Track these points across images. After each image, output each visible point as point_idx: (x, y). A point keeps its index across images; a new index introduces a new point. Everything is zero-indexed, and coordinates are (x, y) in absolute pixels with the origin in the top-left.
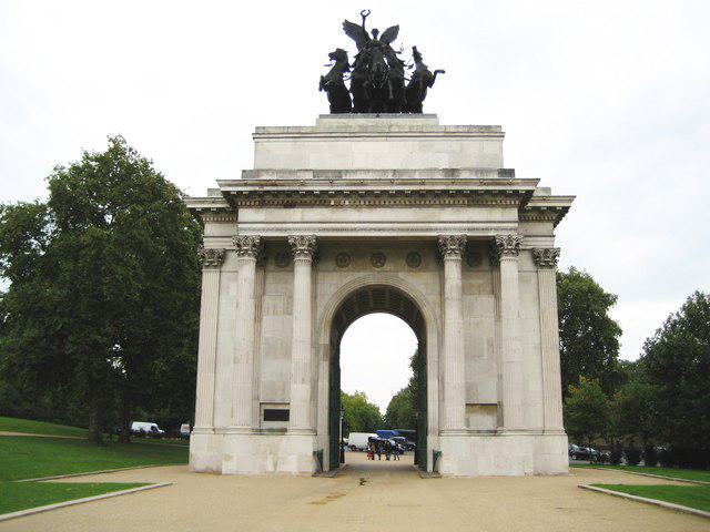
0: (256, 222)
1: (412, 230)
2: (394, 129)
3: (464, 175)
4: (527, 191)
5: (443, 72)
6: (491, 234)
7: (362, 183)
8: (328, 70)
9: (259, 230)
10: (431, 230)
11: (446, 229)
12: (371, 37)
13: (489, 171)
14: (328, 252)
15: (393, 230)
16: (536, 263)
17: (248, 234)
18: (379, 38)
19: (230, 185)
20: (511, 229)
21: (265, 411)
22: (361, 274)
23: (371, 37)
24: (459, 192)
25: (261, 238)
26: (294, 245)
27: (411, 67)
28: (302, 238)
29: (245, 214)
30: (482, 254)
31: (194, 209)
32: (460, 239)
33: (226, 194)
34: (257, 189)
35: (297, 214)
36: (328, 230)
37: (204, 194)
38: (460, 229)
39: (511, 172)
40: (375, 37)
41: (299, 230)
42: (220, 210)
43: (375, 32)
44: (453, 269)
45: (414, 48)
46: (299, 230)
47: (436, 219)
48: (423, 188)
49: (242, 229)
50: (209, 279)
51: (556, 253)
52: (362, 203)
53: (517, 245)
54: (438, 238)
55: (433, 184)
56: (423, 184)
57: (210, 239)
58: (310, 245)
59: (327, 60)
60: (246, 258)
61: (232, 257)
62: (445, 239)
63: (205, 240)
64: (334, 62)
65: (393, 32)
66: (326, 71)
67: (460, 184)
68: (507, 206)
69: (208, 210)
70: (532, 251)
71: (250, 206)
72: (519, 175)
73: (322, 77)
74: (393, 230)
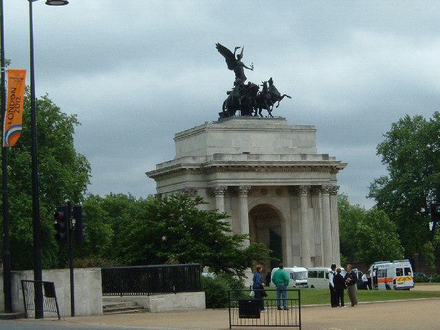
0: (223, 180)
3: (309, 159)
5: (290, 97)
7: (272, 162)
10: (295, 182)
12: (237, 58)
13: (316, 155)
14: (253, 191)
23: (237, 58)
30: (314, 190)
32: (308, 186)
34: (228, 164)
35: (242, 175)
39: (326, 156)
44: (304, 199)
45: (271, 79)
51: (338, 188)
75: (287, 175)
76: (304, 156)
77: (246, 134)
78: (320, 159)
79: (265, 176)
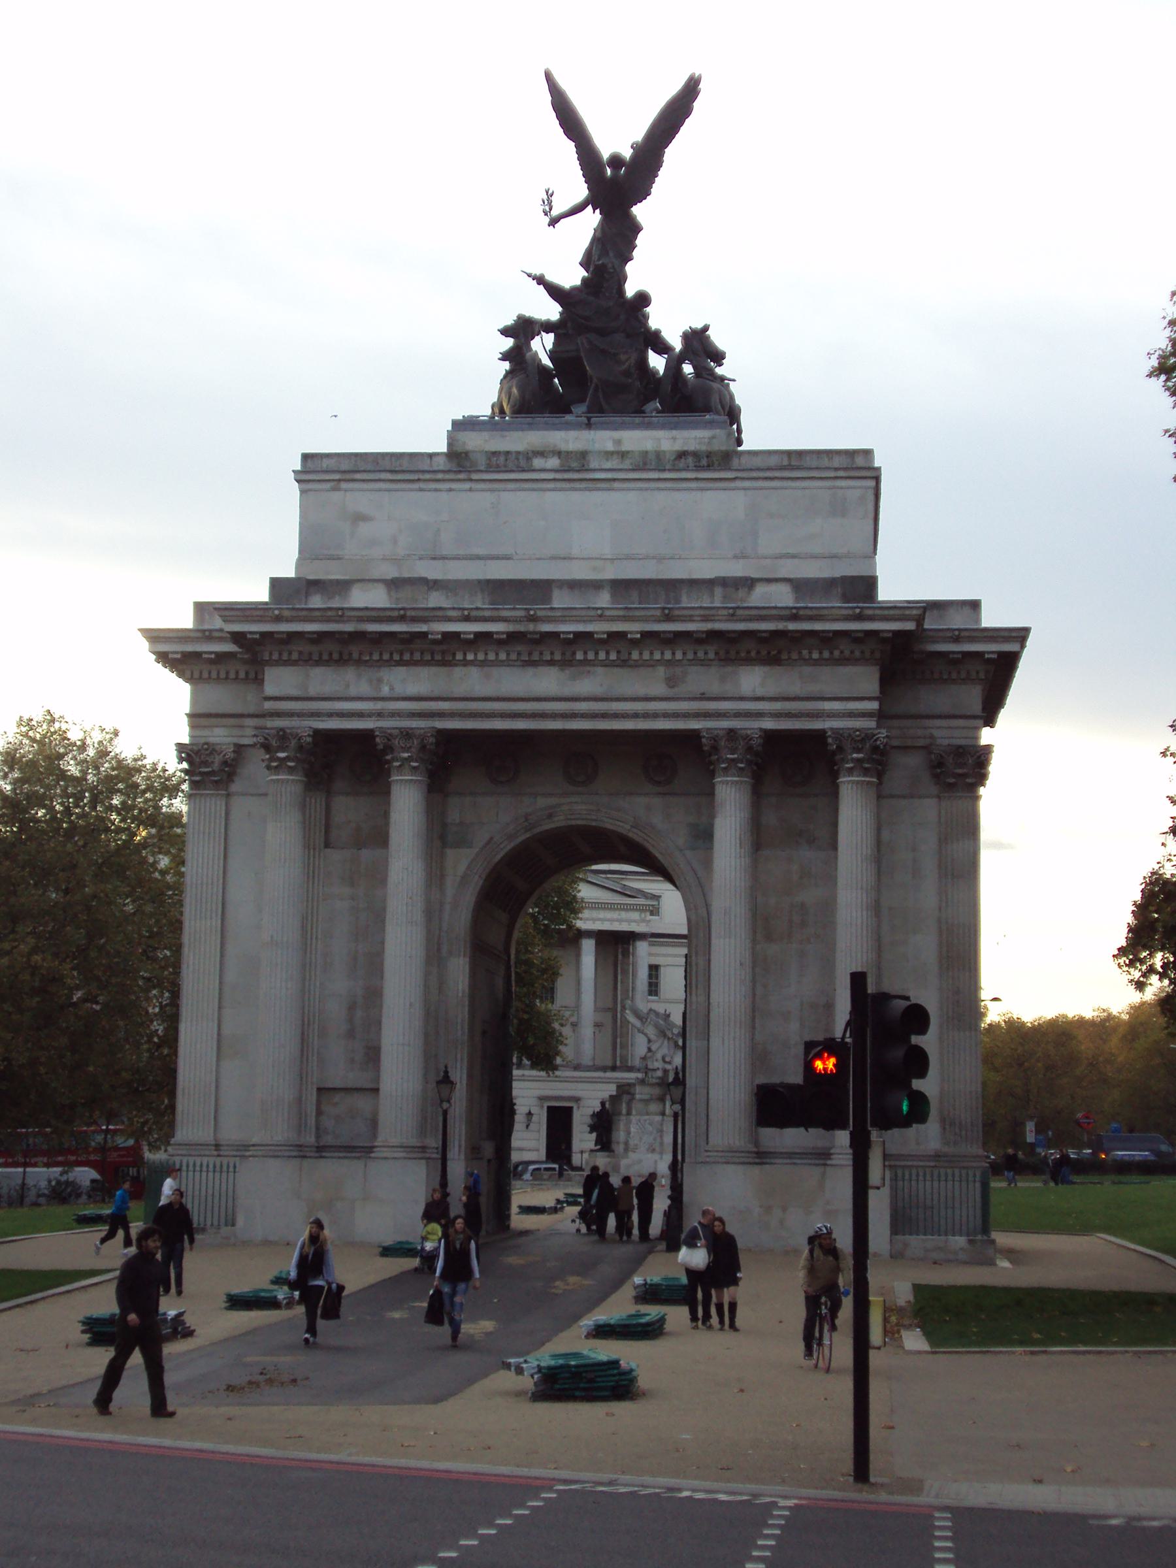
4: (897, 634)
16: (936, 777)
22: (542, 802)
25: (317, 733)
33: (238, 637)
37: (185, 620)
42: (221, 657)
58: (423, 748)
61: (255, 768)
62: (715, 739)
72: (887, 592)
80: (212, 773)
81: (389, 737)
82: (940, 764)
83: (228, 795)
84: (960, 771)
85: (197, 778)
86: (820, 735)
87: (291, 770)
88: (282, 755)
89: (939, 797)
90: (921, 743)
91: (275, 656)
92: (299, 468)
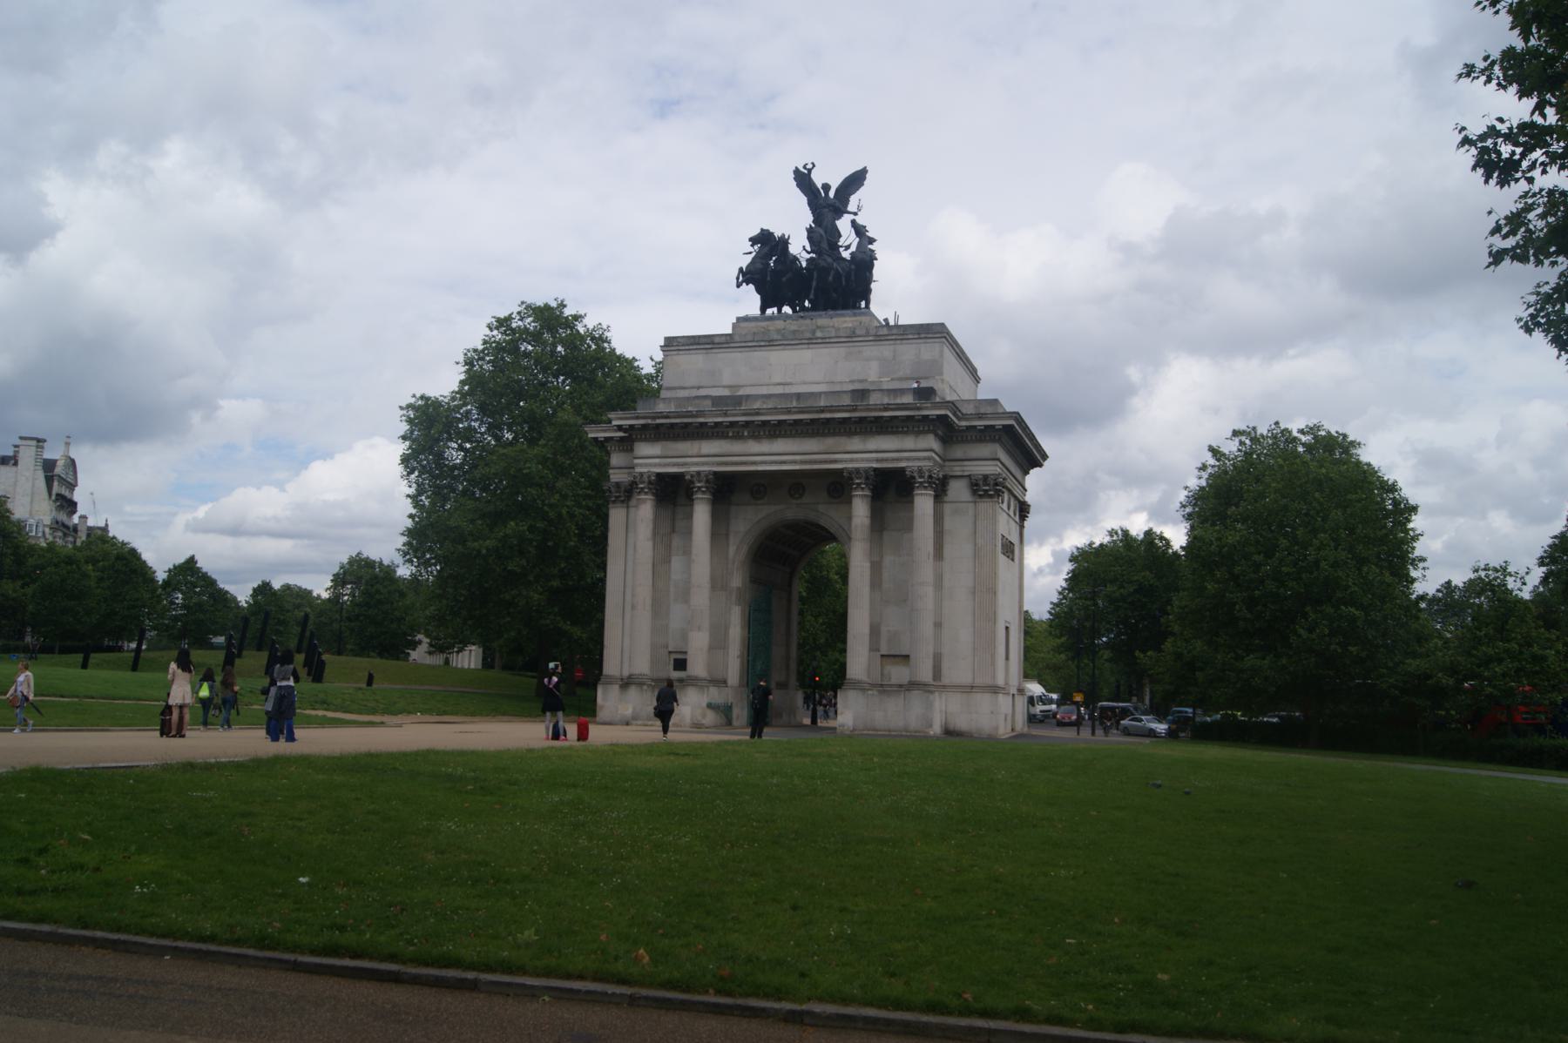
1: (815, 462)
2: (819, 334)
3: (874, 399)
6: (903, 464)
8: (749, 258)
9: (655, 465)
10: (835, 461)
11: (852, 460)
13: (902, 392)
15: (795, 462)
16: (974, 492)
17: (645, 470)
18: (832, 194)
19: (621, 419)
20: (925, 459)
21: (675, 660)
24: (861, 420)
26: (692, 482)
27: (847, 247)
28: (699, 473)
29: (644, 449)
31: (597, 438)
32: (866, 470)
34: (649, 421)
36: (726, 464)
38: (868, 460)
40: (827, 193)
41: (697, 464)
42: (622, 438)
43: (826, 187)
46: (697, 464)
47: (841, 449)
48: (823, 416)
49: (638, 465)
50: (616, 516)
52: (762, 433)
53: (930, 477)
54: (841, 471)
55: (831, 411)
56: (822, 411)
57: (616, 471)
58: (707, 481)
59: (748, 247)
60: (643, 497)
63: (611, 471)
64: (756, 247)
65: (855, 181)
66: (745, 261)
67: (861, 410)
68: (918, 433)
69: (612, 438)
70: (969, 476)
71: (646, 440)
73: (741, 270)
74: (795, 462)
75: (810, 445)
76: (862, 394)
77: (759, 355)
78: (908, 399)
79: (753, 446)
80: (620, 496)
81: (692, 476)
82: (977, 485)
83: (628, 507)
84: (984, 488)
85: (613, 499)
86: (903, 470)
87: (646, 493)
88: (642, 486)
89: (975, 502)
90: (966, 473)
91: (639, 437)
92: (663, 344)
